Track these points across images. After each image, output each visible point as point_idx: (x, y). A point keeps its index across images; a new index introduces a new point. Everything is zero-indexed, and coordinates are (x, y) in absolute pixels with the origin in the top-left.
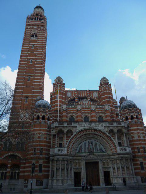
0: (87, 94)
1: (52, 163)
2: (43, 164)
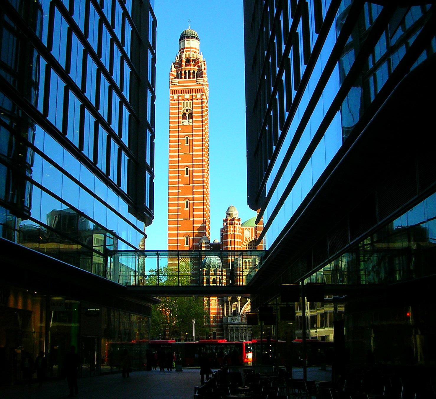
2: (217, 332)
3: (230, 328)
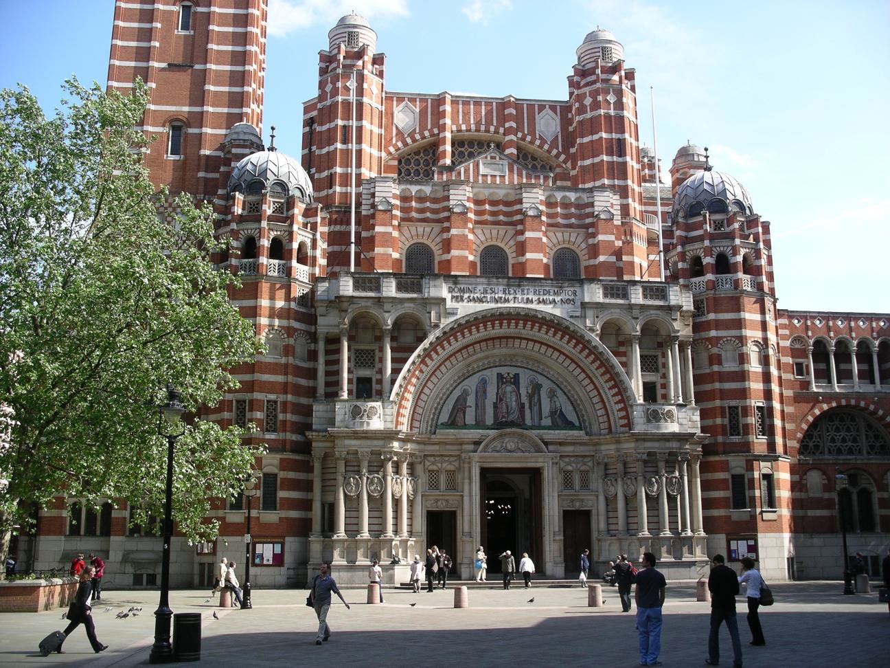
0: (503, 119)
1: (323, 468)
2: (282, 475)
3: (344, 454)
